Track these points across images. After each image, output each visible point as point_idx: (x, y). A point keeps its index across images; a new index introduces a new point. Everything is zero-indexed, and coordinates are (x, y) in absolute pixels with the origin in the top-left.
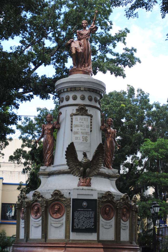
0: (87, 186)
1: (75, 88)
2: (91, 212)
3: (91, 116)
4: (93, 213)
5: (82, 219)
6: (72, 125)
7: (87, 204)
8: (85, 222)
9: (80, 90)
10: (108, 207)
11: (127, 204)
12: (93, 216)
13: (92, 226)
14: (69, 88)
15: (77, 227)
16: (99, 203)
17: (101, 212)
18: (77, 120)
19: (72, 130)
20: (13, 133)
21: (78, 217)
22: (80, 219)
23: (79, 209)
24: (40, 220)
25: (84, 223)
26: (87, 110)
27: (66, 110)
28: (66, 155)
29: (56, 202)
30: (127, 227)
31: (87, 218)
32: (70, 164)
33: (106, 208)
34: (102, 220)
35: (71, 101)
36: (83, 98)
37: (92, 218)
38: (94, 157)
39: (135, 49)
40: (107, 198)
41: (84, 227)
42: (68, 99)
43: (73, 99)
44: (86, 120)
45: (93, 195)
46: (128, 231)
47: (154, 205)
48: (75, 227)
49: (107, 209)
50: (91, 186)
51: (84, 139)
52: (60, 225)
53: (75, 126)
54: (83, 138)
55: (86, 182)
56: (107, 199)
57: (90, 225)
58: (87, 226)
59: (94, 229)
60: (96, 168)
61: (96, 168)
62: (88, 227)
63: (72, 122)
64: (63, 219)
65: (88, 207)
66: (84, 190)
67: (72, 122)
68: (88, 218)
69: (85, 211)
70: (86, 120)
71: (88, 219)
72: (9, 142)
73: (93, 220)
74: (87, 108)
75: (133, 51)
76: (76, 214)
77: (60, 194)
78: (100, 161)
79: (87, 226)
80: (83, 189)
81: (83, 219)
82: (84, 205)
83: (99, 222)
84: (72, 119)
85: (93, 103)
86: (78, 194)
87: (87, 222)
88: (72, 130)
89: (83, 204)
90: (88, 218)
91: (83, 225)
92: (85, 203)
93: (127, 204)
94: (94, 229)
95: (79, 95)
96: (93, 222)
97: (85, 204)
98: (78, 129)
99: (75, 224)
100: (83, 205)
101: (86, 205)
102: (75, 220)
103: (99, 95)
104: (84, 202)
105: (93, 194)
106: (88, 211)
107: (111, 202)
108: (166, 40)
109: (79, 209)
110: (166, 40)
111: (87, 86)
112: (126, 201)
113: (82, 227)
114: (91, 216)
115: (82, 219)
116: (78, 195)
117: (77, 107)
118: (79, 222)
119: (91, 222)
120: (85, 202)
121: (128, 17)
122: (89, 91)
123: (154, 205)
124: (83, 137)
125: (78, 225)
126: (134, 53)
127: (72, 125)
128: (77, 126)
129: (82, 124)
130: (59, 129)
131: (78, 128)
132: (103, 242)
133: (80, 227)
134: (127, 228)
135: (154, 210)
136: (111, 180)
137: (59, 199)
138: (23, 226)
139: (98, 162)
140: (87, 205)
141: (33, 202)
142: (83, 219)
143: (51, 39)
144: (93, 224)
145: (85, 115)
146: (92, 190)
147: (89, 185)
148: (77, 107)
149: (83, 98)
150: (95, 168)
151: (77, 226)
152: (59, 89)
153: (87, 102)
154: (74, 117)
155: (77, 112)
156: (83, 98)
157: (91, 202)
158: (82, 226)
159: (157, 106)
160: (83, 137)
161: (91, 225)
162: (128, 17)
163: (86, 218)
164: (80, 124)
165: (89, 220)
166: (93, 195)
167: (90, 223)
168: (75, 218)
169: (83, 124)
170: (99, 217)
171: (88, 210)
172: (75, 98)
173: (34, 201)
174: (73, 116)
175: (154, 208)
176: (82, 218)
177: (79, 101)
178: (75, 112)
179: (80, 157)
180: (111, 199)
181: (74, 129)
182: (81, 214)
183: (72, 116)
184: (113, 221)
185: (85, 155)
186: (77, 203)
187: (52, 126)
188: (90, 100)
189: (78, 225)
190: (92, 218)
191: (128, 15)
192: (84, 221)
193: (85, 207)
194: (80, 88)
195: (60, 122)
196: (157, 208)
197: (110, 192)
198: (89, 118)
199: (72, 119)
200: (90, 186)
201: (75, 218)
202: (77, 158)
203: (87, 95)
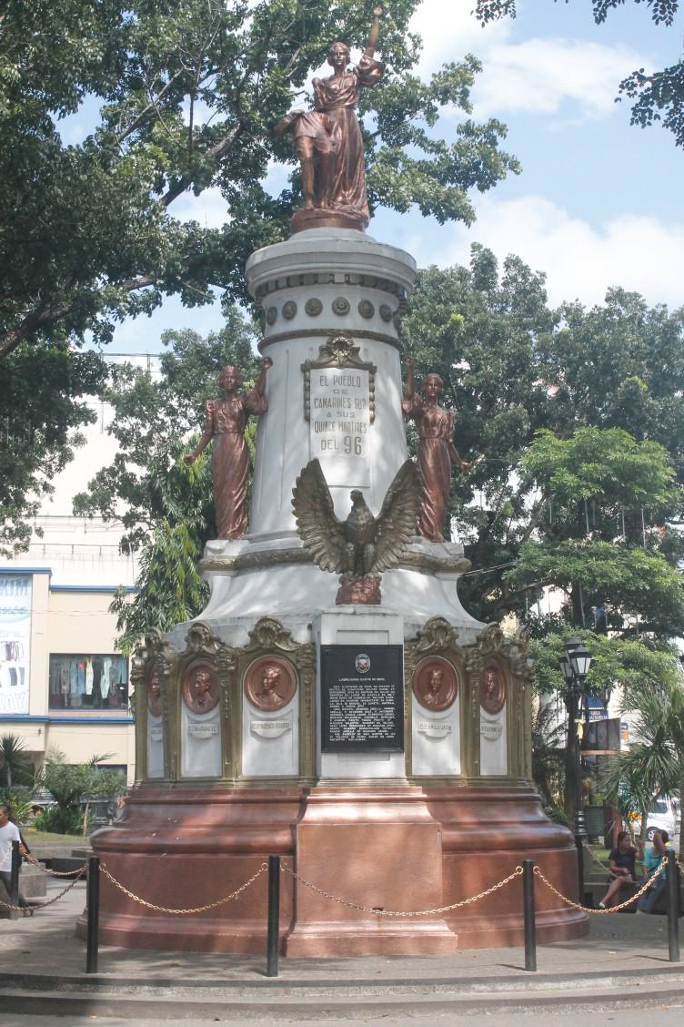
0: (367, 602)
1: (316, 275)
2: (385, 688)
3: (371, 369)
4: (389, 689)
5: (355, 709)
6: (307, 399)
7: (369, 661)
8: (367, 721)
9: (333, 281)
11: (498, 656)
12: (390, 701)
13: (390, 732)
14: (294, 276)
15: (339, 739)
17: (415, 686)
18: (323, 382)
19: (307, 419)
20: (89, 422)
21: (341, 707)
22: (348, 712)
23: (345, 680)
24: (215, 717)
25: (361, 722)
26: (358, 349)
27: (288, 352)
28: (294, 503)
29: (268, 657)
30: (500, 730)
31: (373, 706)
32: (309, 532)
33: (431, 674)
35: (302, 321)
37: (387, 706)
38: (387, 511)
40: (433, 640)
42: (290, 314)
43: (308, 313)
44: (355, 383)
45: (387, 631)
46: (502, 742)
47: (570, 651)
48: (335, 737)
50: (382, 602)
51: (350, 446)
53: (317, 403)
54: (345, 444)
55: (362, 591)
57: (381, 728)
58: (371, 734)
59: (395, 740)
60: (393, 544)
61: (393, 544)
62: (375, 736)
63: (307, 389)
65: (374, 671)
67: (307, 389)
68: (376, 706)
69: (363, 683)
70: (355, 383)
71: (373, 709)
72: (73, 449)
73: (390, 712)
74: (358, 343)
75: (495, 133)
76: (335, 694)
77: (278, 630)
78: (408, 518)
79: (371, 734)
80: (354, 614)
81: (359, 710)
82: (359, 664)
84: (307, 380)
85: (376, 325)
87: (372, 720)
88: (307, 419)
89: (357, 662)
90: (376, 706)
91: (357, 728)
93: (498, 656)
94: (395, 740)
95: (327, 298)
96: (392, 720)
97: (363, 662)
98: (329, 415)
99: (333, 729)
100: (357, 665)
101: (366, 664)
102: (333, 715)
103: (393, 296)
104: (361, 656)
106: (372, 683)
107: (450, 650)
108: (616, 100)
109: (345, 680)
110: (616, 100)
111: (355, 269)
112: (494, 647)
113: (356, 736)
114: (385, 699)
116: (340, 633)
117: (322, 341)
118: (347, 720)
119: (386, 720)
120: (366, 656)
121: (483, 20)
123: (570, 651)
124: (348, 439)
125: (342, 730)
126: (499, 139)
127: (307, 399)
128: (324, 403)
129: (340, 396)
130: (262, 414)
131: (329, 410)
132: (424, 782)
133: (350, 737)
134: (500, 735)
135: (572, 668)
136: (439, 578)
137: (277, 648)
138: (160, 737)
139: (402, 522)
140: (369, 665)
141: (188, 658)
142: (359, 710)
143: (214, 97)
144: (391, 725)
145: (352, 364)
146: (384, 615)
147: (375, 599)
148: (322, 341)
149: (341, 309)
150: (390, 542)
151: (341, 735)
153: (353, 321)
154: (314, 374)
155: (321, 356)
156: (344, 308)
157: (385, 658)
158: (356, 731)
159: (573, 313)
160: (348, 439)
161: (383, 732)
162: (483, 20)
163: (367, 706)
164: (336, 396)
165: (378, 712)
167: (382, 723)
168: (332, 709)
169: (345, 396)
171: (374, 679)
172: (314, 309)
173: (193, 655)
175: (573, 660)
176: (357, 706)
177: (327, 320)
178: (315, 357)
179: (343, 507)
180: (445, 642)
181: (316, 413)
182: (350, 695)
183: (309, 370)
184: (454, 714)
185: (357, 498)
186: (338, 661)
188: (367, 312)
190: (387, 706)
191: (484, 12)
192: (363, 717)
193: (363, 672)
194: (332, 275)
195: (267, 390)
196: (581, 661)
197: (444, 620)
198: (365, 375)
199: (307, 380)
200: (379, 602)
201: (332, 709)
202: (333, 513)
203: (355, 297)
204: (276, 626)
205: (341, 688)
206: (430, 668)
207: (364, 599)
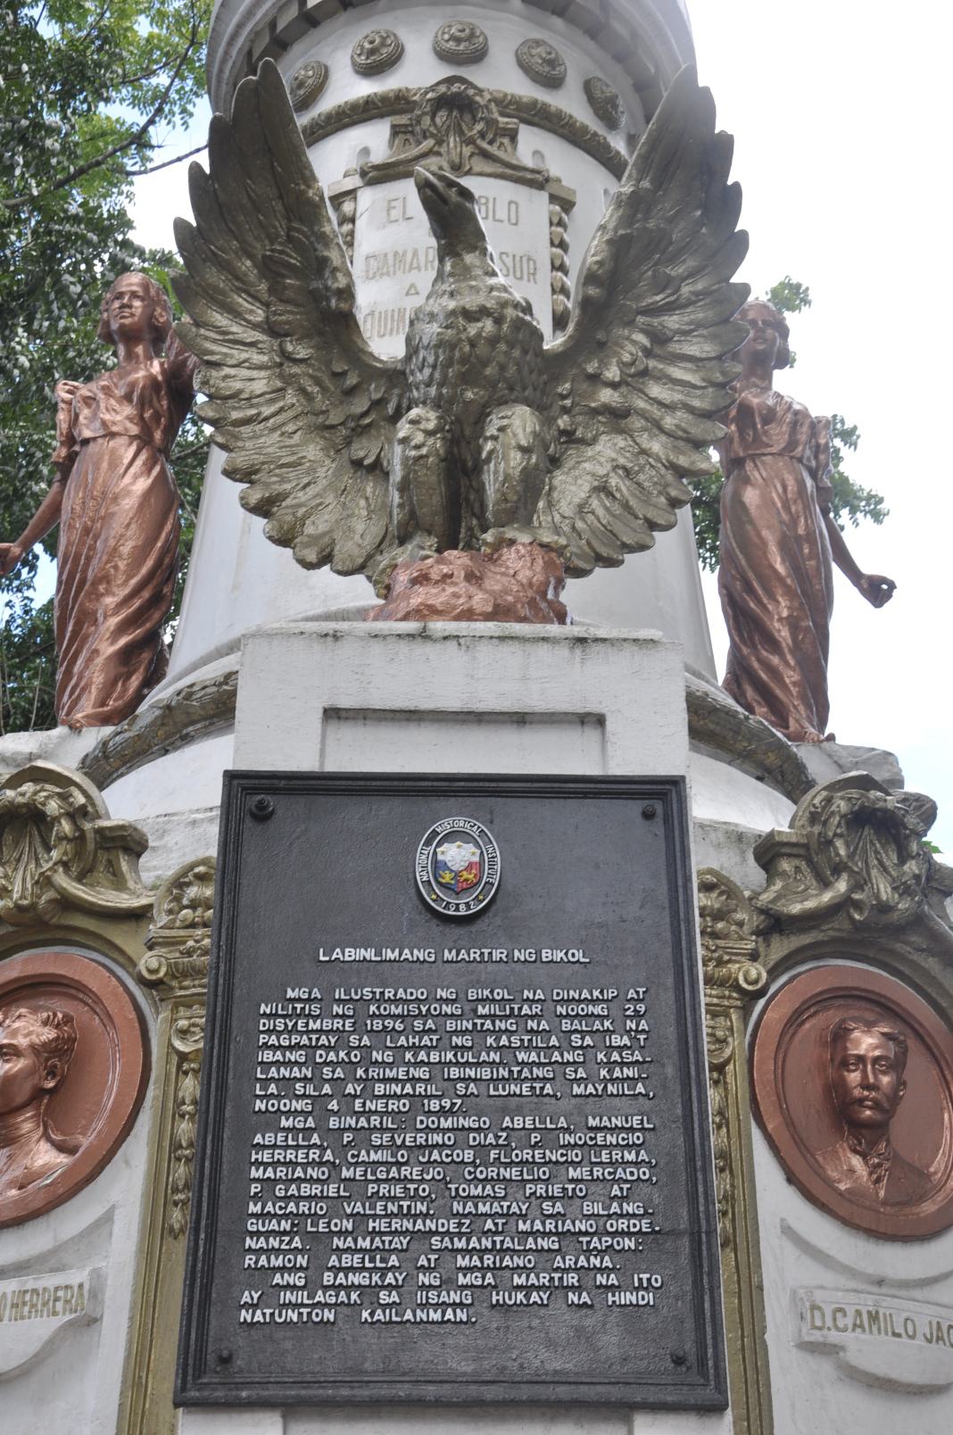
5: (404, 1121)
10: (869, 1025)
13: (626, 1263)
16: (719, 915)
18: (395, 214)
23: (351, 954)
33: (840, 1036)
34: (788, 1231)
35: (348, 88)
36: (458, 40)
39: (848, 425)
40: (838, 869)
41: (448, 1283)
45: (600, 720)
49: (866, 1042)
52: (42, 1328)
56: (842, 886)
64: (107, 1218)
66: (452, 645)
82: (438, 866)
83: (746, 1244)
86: (333, 714)
89: (422, 858)
92: (451, 837)
97: (457, 855)
100: (422, 876)
104: (444, 826)
105: (593, 707)
109: (351, 954)
115: (404, 1121)
122: (583, 723)
125: (318, 1244)
126: (845, 451)
137: (68, 904)
145: (500, 169)
152: (240, 26)
166: (600, 720)
168: (270, 1121)
170: (736, 1164)
172: (377, 62)
174: (359, 193)
187: (156, 368)
189: (318, 1244)
201: (270, 1121)
204: (64, 797)
205: (327, 1001)
206: (830, 1018)
207: (480, 601)
